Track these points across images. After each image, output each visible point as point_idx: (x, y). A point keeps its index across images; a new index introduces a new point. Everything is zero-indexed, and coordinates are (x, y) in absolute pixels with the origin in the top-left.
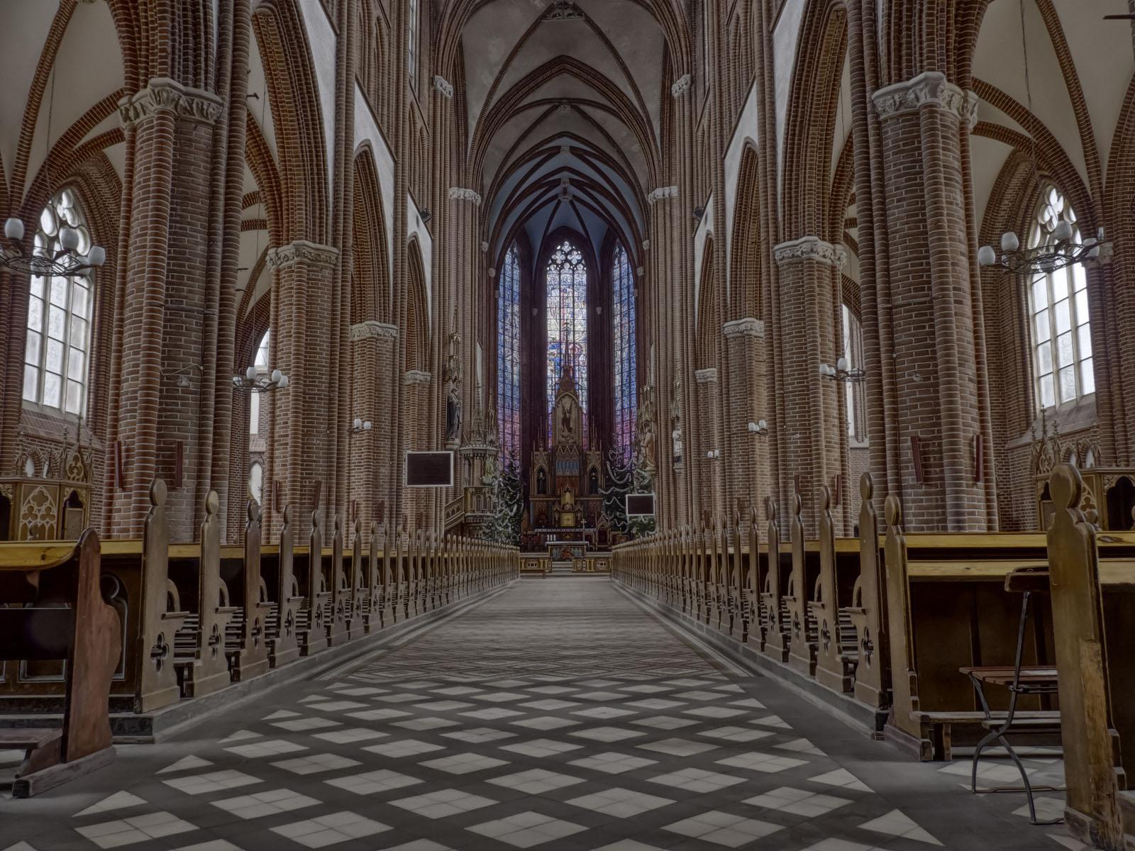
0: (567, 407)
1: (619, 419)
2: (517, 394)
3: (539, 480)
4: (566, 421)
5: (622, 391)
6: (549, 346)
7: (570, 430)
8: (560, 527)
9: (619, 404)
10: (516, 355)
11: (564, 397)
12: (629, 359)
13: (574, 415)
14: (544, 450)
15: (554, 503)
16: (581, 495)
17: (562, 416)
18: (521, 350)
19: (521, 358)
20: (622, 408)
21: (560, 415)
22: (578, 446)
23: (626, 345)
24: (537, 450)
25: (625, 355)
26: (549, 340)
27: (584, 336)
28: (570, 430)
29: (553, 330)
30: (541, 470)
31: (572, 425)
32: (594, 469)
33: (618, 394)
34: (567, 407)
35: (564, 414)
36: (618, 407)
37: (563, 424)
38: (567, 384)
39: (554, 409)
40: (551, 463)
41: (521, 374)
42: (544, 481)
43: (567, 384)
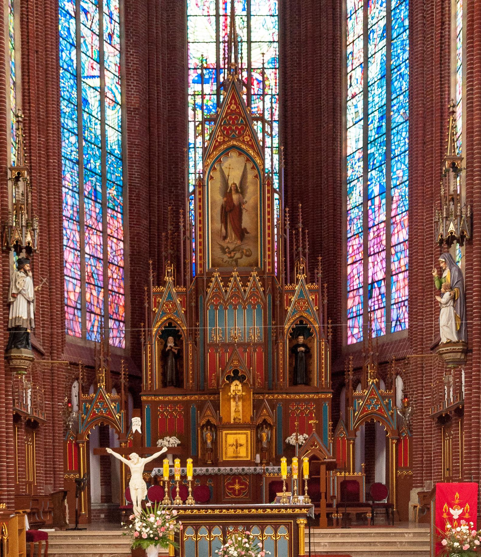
0: (234, 178)
1: (354, 226)
2: (116, 173)
3: (164, 355)
4: (231, 212)
5: (366, 158)
6: (193, 75)
7: (241, 234)
8: (215, 463)
9: (359, 187)
10: (112, 82)
11: (226, 153)
12: (387, 75)
13: (251, 197)
14: (177, 283)
15: (201, 406)
16: (269, 386)
17: (220, 199)
18: (126, 75)
19: (126, 93)
20: (367, 197)
21: (214, 195)
22: (261, 273)
23: (378, 46)
24: (160, 282)
25: (374, 71)
26: (192, 62)
27: (273, 52)
28: (241, 234)
29: (201, 42)
30: (169, 331)
31: (246, 222)
32: (302, 329)
33: (354, 168)
34: (234, 178)
35: (227, 193)
36: (355, 198)
37: (224, 221)
38: (233, 123)
39: (200, 183)
40: (195, 313)
41: (127, 128)
42: (179, 357)
43: (233, 123)
